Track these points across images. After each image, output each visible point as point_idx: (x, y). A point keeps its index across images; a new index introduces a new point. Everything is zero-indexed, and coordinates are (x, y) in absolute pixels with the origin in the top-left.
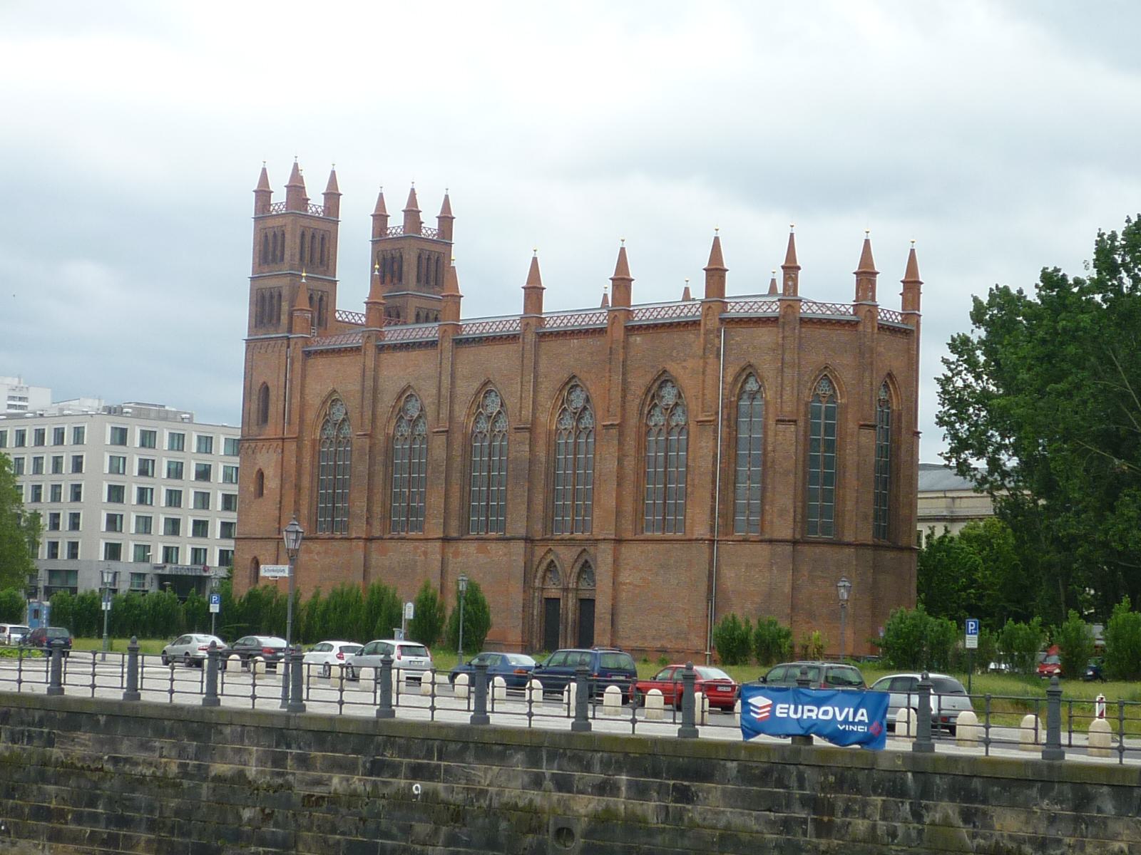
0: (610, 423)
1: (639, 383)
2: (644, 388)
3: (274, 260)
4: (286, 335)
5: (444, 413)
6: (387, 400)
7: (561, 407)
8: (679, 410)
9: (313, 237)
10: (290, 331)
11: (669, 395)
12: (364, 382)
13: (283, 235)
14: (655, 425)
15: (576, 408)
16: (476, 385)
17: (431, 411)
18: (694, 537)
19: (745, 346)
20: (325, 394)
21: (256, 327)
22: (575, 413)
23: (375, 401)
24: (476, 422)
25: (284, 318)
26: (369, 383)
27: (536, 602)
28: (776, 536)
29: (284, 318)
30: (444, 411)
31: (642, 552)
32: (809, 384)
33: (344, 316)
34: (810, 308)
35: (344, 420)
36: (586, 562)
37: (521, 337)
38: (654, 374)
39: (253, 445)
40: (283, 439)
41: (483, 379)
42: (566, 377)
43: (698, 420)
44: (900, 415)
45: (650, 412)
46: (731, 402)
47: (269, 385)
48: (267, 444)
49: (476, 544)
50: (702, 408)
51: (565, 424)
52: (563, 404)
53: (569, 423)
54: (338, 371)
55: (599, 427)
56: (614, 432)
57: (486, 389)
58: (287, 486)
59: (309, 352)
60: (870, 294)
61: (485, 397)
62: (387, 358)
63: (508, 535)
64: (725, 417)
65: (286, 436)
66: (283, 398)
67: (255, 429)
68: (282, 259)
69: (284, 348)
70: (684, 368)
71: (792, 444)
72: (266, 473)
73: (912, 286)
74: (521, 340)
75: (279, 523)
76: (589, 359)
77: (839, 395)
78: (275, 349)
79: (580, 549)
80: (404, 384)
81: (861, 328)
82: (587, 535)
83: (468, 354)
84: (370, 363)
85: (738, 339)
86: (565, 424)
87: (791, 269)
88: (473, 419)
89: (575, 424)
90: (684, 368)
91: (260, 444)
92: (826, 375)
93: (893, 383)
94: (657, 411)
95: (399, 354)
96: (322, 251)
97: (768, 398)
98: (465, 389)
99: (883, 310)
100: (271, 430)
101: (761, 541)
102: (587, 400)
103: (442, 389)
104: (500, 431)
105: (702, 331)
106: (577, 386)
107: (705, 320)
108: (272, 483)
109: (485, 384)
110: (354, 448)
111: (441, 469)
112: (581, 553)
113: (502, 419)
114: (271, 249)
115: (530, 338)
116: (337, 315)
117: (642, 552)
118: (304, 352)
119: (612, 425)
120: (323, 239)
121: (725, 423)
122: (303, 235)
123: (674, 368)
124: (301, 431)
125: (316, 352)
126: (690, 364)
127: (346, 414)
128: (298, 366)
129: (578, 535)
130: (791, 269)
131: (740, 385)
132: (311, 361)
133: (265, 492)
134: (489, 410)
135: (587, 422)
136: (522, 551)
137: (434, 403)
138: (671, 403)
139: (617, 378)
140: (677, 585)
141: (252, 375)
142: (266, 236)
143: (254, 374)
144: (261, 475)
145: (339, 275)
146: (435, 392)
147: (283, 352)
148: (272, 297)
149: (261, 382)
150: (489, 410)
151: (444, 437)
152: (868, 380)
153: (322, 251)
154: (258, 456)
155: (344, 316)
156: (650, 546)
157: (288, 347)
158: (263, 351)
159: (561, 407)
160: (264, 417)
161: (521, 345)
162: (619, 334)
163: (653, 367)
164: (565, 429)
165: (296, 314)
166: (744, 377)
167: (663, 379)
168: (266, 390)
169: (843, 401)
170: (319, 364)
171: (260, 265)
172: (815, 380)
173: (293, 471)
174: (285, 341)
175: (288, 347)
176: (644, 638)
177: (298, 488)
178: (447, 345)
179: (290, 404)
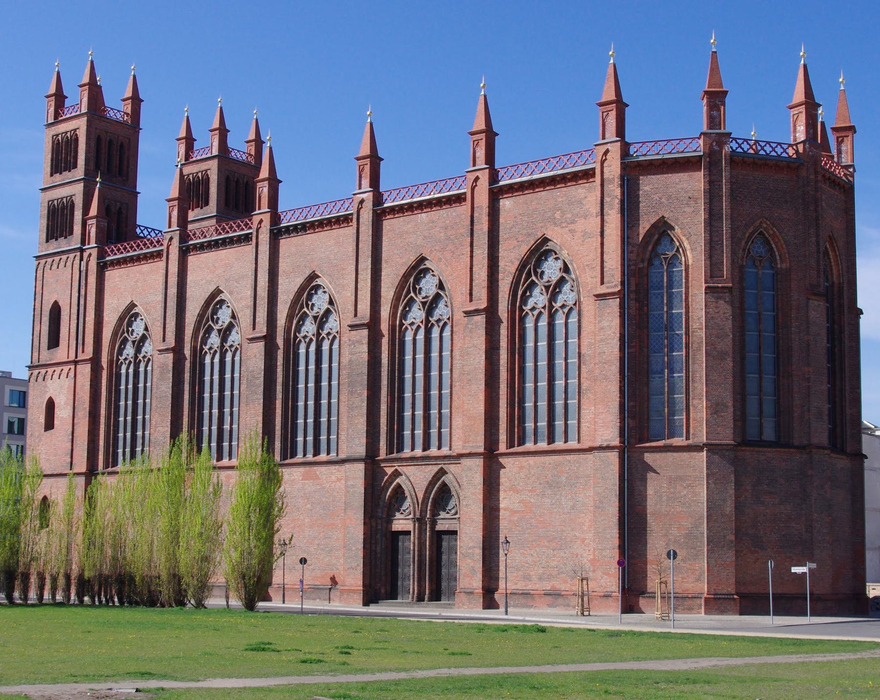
2: (517, 263)
4: (79, 246)
7: (406, 297)
8: (566, 288)
9: (110, 142)
11: (551, 270)
15: (426, 297)
16: (299, 281)
18: (597, 444)
19: (656, 197)
21: (47, 241)
22: (426, 302)
26: (173, 291)
27: (379, 536)
31: (521, 468)
32: (743, 243)
36: (444, 485)
39: (43, 371)
41: (308, 273)
42: (411, 259)
44: (841, 289)
45: (524, 292)
46: (639, 268)
47: (60, 304)
48: (58, 369)
49: (302, 469)
53: (417, 314)
54: (137, 281)
55: (459, 316)
56: (481, 319)
63: (342, 456)
64: (633, 288)
65: (79, 359)
69: (77, 261)
71: (727, 319)
75: (72, 457)
76: (442, 235)
77: (778, 258)
78: (69, 264)
79: (436, 469)
80: (212, 288)
81: (804, 173)
82: (445, 451)
85: (646, 188)
89: (424, 315)
91: (50, 370)
92: (761, 232)
93: (834, 251)
94: (536, 291)
96: (121, 161)
97: (690, 262)
98: (287, 289)
100: (61, 353)
108: (62, 413)
109: (313, 276)
110: (155, 367)
111: (257, 382)
112: (437, 473)
115: (367, 216)
116: (138, 231)
117: (521, 468)
120: (122, 146)
121: (632, 296)
122: (99, 139)
123: (557, 237)
126: (580, 226)
129: (433, 451)
131: (650, 248)
135: (441, 311)
136: (362, 474)
138: (555, 279)
140: (573, 507)
144: (51, 406)
145: (141, 186)
146: (249, 293)
147: (76, 266)
149: (52, 302)
151: (261, 345)
152: (814, 239)
153: (121, 161)
155: (146, 233)
156: (531, 460)
157: (81, 259)
159: (406, 297)
161: (355, 225)
165: (89, 222)
166: (656, 237)
168: (56, 311)
169: (784, 266)
171: (52, 175)
172: (750, 237)
175: (81, 259)
176: (527, 578)
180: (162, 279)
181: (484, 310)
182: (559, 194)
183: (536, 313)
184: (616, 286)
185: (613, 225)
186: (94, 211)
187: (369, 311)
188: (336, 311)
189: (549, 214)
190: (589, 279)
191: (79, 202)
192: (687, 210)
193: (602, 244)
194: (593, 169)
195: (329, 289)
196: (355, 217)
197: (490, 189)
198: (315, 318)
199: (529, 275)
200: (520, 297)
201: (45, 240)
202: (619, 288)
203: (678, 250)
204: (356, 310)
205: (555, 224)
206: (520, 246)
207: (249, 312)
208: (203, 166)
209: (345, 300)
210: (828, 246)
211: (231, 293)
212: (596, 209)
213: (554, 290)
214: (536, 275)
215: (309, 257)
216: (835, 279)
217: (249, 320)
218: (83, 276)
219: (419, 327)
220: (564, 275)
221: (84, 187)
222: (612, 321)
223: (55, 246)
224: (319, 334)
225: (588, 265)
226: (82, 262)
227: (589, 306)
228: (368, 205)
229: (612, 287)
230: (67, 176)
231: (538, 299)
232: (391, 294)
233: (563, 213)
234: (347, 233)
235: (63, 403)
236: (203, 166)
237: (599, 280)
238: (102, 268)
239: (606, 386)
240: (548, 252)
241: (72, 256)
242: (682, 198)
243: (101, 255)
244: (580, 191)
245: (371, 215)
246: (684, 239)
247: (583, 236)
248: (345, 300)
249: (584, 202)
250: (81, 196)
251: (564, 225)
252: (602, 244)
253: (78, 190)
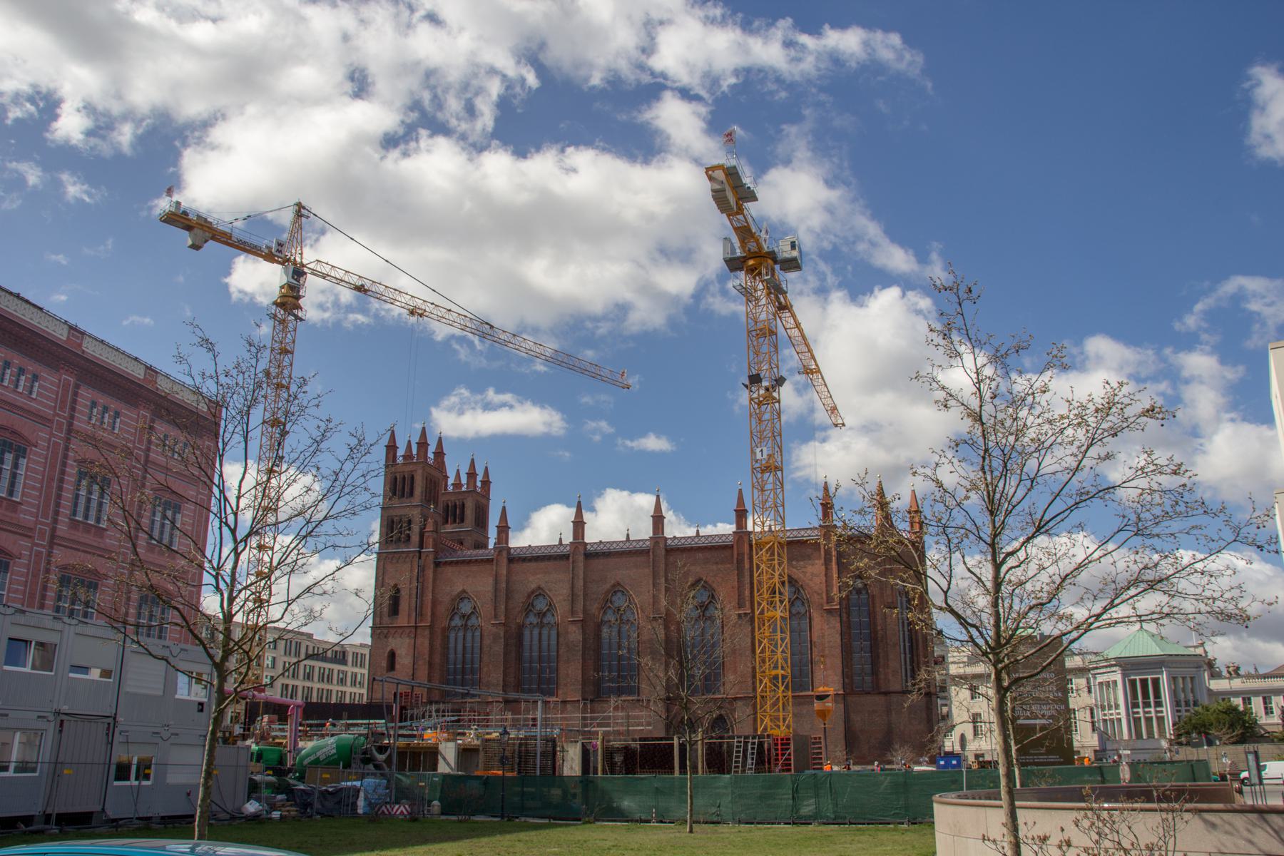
3: (403, 496)
5: (579, 606)
6: (519, 599)
10: (421, 546)
13: (412, 478)
23: (508, 597)
24: (605, 613)
25: (415, 538)
28: (892, 689)
35: (472, 613)
39: (385, 631)
40: (416, 627)
48: (400, 631)
58: (420, 663)
59: (440, 562)
61: (612, 595)
62: (517, 567)
67: (386, 619)
68: (411, 494)
69: (416, 559)
72: (398, 652)
74: (651, 553)
83: (598, 564)
88: (602, 612)
91: (392, 631)
95: (528, 564)
100: (402, 620)
101: (880, 693)
108: (404, 659)
114: (399, 487)
118: (435, 562)
120: (435, 483)
124: (432, 621)
125: (446, 563)
127: (475, 608)
132: (440, 569)
133: (397, 666)
137: (565, 600)
142: (396, 478)
144: (392, 655)
146: (565, 591)
150: (616, 605)
154: (390, 639)
157: (420, 558)
160: (394, 609)
165: (426, 534)
170: (449, 571)
173: (426, 651)
174: (417, 554)
175: (420, 558)
177: (431, 665)
235: (404, 653)
241: (411, 555)
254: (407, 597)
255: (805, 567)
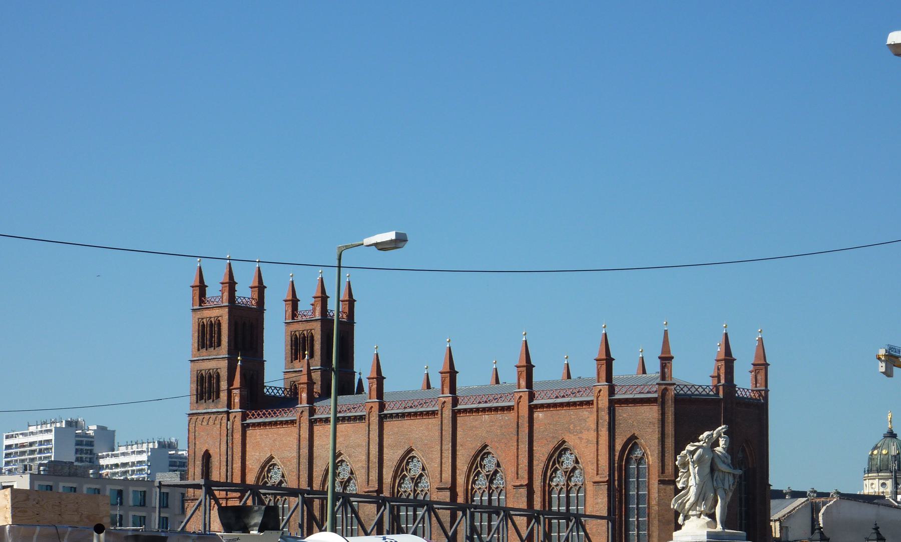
0: (519, 484)
1: (542, 452)
2: (547, 456)
3: (211, 346)
4: (225, 409)
5: (374, 475)
7: (475, 470)
11: (568, 461)
12: (299, 449)
14: (557, 485)
15: (489, 471)
16: (401, 452)
17: (360, 476)
19: (630, 421)
20: (263, 460)
22: (487, 476)
25: (224, 396)
26: (305, 451)
29: (224, 396)
30: (374, 475)
33: (270, 391)
34: (682, 389)
37: (440, 412)
38: (555, 443)
41: (407, 447)
42: (479, 445)
43: (594, 480)
45: (552, 474)
47: (211, 452)
50: (597, 471)
51: (479, 484)
52: (477, 467)
53: (482, 482)
54: (274, 440)
55: (510, 487)
56: (524, 491)
57: (408, 456)
60: (730, 376)
66: (225, 464)
68: (219, 344)
69: (225, 421)
70: (580, 438)
73: (761, 367)
78: (217, 422)
84: (305, 434)
86: (479, 484)
87: (666, 360)
89: (488, 484)
90: (580, 438)
97: (651, 463)
98: (392, 457)
99: (739, 389)
102: (498, 465)
103: (371, 456)
104: (422, 491)
105: (595, 409)
106: (489, 453)
107: (597, 400)
109: (410, 450)
113: (425, 480)
115: (447, 413)
116: (265, 390)
119: (521, 486)
126: (585, 435)
128: (238, 436)
130: (666, 360)
134: (412, 473)
135: (498, 482)
138: (570, 467)
139: (524, 447)
141: (195, 443)
142: (203, 325)
143: (197, 443)
146: (364, 457)
147: (224, 424)
148: (210, 377)
149: (204, 450)
157: (228, 420)
158: (205, 423)
159: (475, 470)
162: (524, 411)
163: (554, 438)
164: (480, 488)
165: (235, 391)
167: (561, 449)
168: (207, 456)
171: (199, 350)
175: (228, 420)
178: (374, 419)
179: (232, 469)
180: (295, 442)
181: (526, 485)
182: (572, 412)
183: (559, 488)
184: (606, 477)
185: (604, 438)
186: (237, 382)
187: (450, 479)
188: (426, 475)
189: (567, 425)
190: (590, 470)
191: (224, 374)
192: (649, 430)
193: (597, 450)
194: (593, 401)
195: (422, 460)
196: (440, 412)
197: (529, 405)
198: (412, 479)
199: (554, 464)
200: (547, 478)
201: (195, 401)
202: (607, 479)
203: (643, 455)
204: (441, 478)
205: (571, 433)
206: (548, 444)
207: (364, 471)
208: (308, 326)
209: (433, 467)
210: (745, 445)
211: (350, 456)
212: (594, 426)
213: (570, 474)
214: (559, 463)
215: (407, 437)
216: (750, 466)
217: (364, 477)
218: (230, 434)
219: (484, 491)
220: (575, 465)
221: (228, 363)
222: (603, 499)
223: (205, 407)
224: (415, 491)
225: (590, 461)
226: (229, 422)
227: (590, 487)
228: (449, 406)
229: (603, 477)
230: (212, 353)
231: (559, 479)
232: (465, 468)
233: (575, 426)
234: (434, 422)
236: (308, 326)
237: (595, 472)
238: (245, 428)
239: (600, 539)
240: (566, 449)
241: (220, 416)
242: (646, 423)
243: (244, 418)
244: (585, 413)
245: (451, 413)
246: (647, 448)
247: (587, 442)
248: (433, 467)
249: (587, 420)
250: (226, 370)
251: (575, 434)
252: (597, 450)
253: (223, 366)
254: (217, 464)
255: (581, 432)
